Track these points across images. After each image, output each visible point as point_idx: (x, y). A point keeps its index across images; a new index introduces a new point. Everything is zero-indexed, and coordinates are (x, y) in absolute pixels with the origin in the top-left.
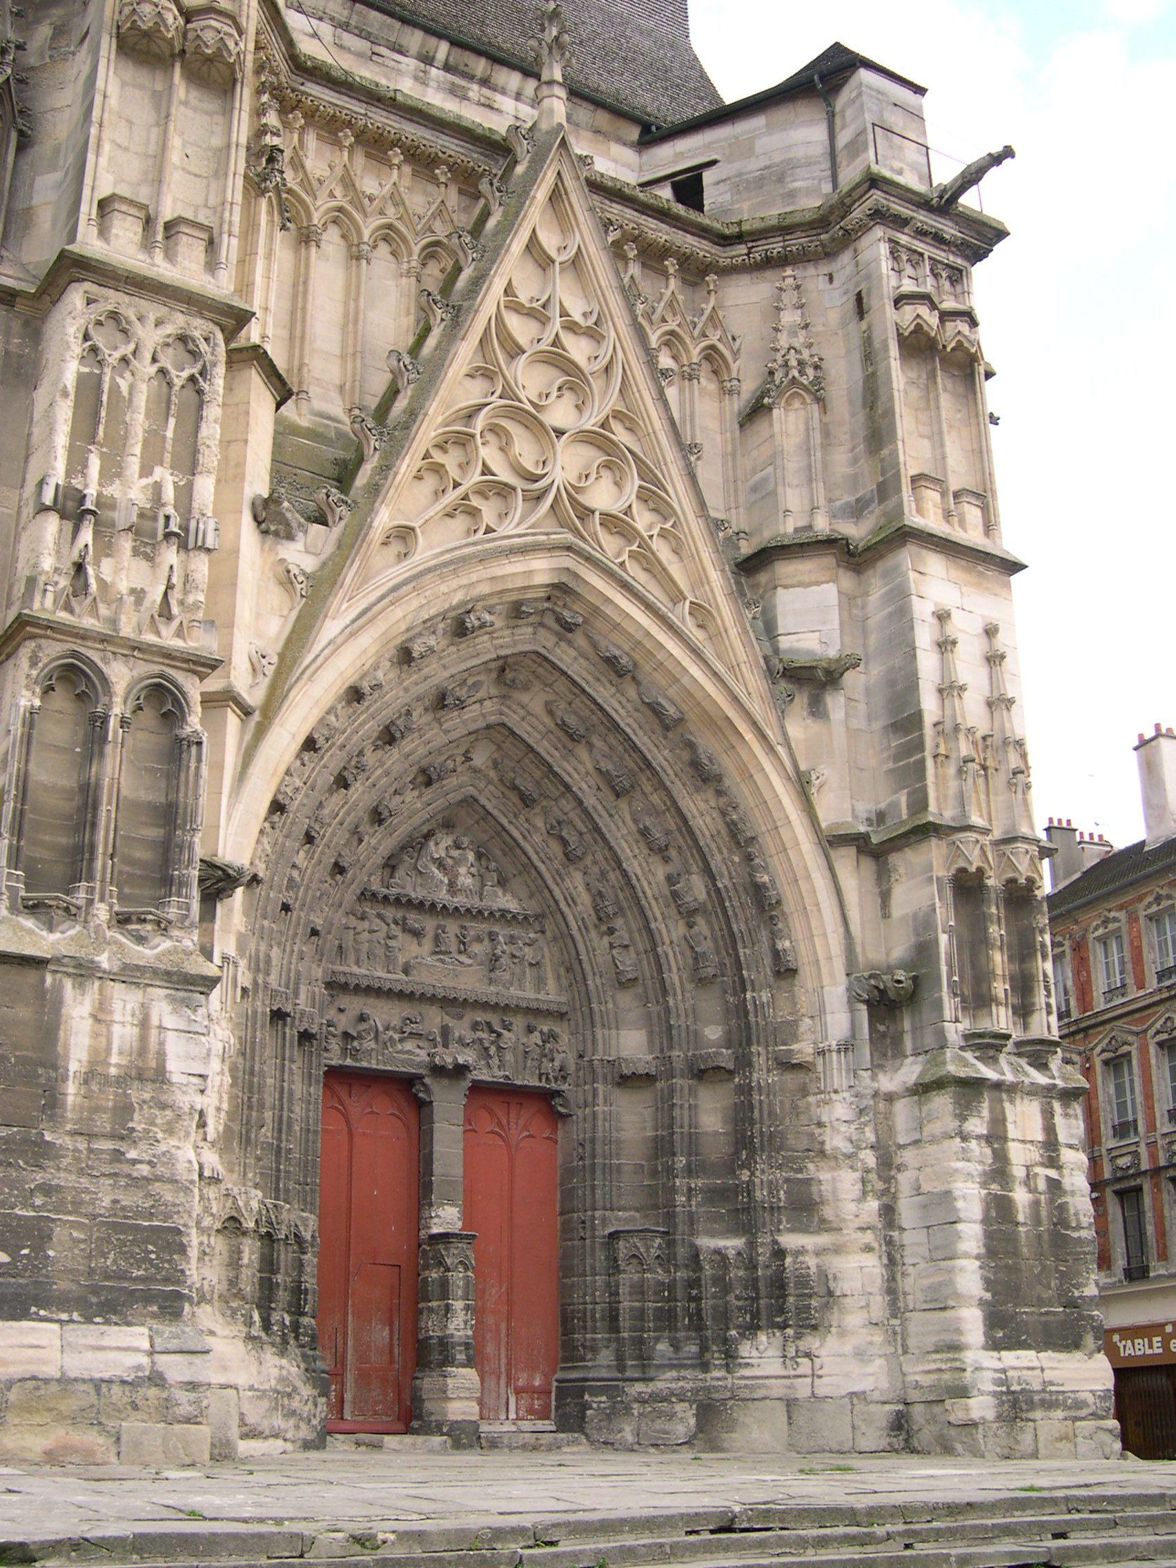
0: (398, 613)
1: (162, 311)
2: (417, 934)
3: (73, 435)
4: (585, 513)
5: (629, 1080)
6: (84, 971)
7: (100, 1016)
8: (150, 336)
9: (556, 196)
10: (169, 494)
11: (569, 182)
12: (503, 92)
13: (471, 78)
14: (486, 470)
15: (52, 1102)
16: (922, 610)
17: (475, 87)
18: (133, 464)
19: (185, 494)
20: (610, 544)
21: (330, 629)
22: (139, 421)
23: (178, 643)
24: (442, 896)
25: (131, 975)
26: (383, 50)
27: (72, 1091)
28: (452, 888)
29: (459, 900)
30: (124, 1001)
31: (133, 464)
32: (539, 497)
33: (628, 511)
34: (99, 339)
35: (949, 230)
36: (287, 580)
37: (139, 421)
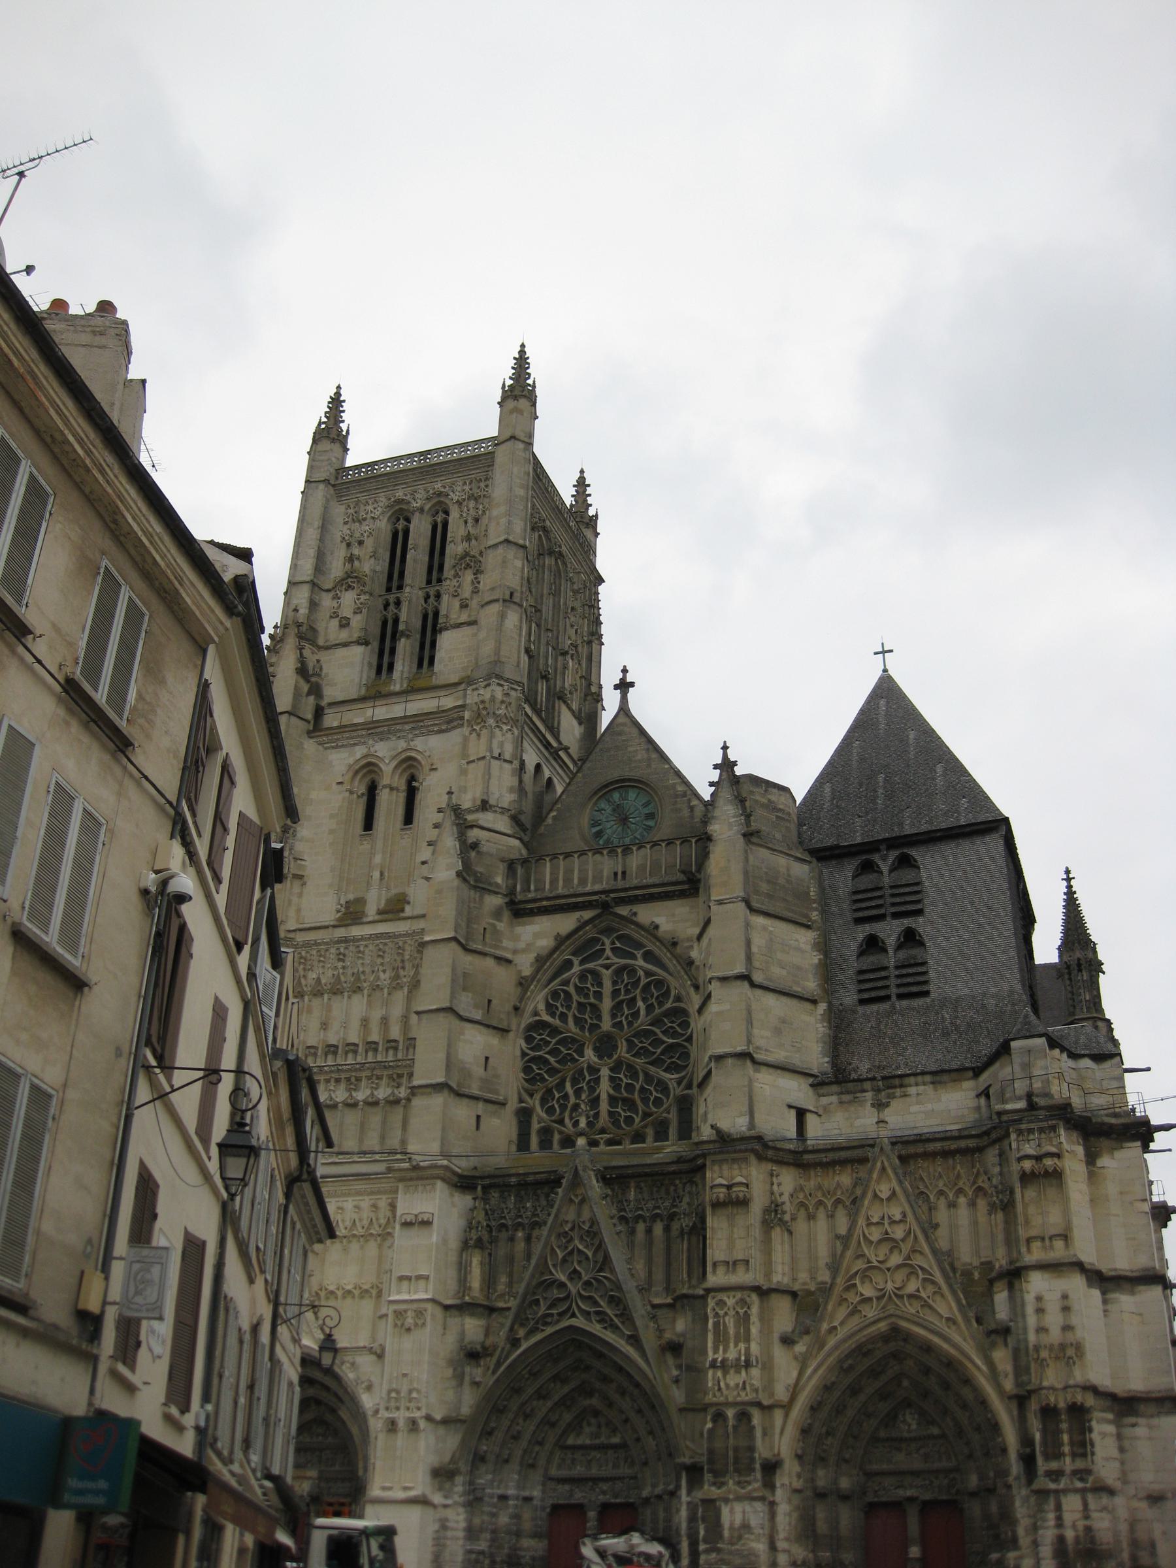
0: (831, 1359)
1: (732, 1293)
2: (899, 1450)
3: (714, 1343)
4: (900, 1297)
5: (973, 1494)
6: (726, 1500)
7: (732, 1511)
8: (730, 1302)
9: (883, 1169)
10: (743, 1352)
11: (886, 1164)
12: (910, 1086)
13: (895, 1087)
14: (862, 1295)
15: (721, 1536)
16: (1030, 1298)
17: (898, 1090)
18: (732, 1345)
19: (748, 1350)
20: (911, 1308)
21: (809, 1371)
22: (732, 1331)
23: (747, 1398)
24: (906, 1435)
25: (739, 1499)
26: (858, 1095)
27: (726, 1533)
28: (909, 1431)
29: (913, 1435)
30: (738, 1507)
31: (732, 1345)
32: (884, 1295)
33: (918, 1291)
34: (717, 1310)
35: (1042, 1114)
36: (796, 1358)
37: (732, 1331)
